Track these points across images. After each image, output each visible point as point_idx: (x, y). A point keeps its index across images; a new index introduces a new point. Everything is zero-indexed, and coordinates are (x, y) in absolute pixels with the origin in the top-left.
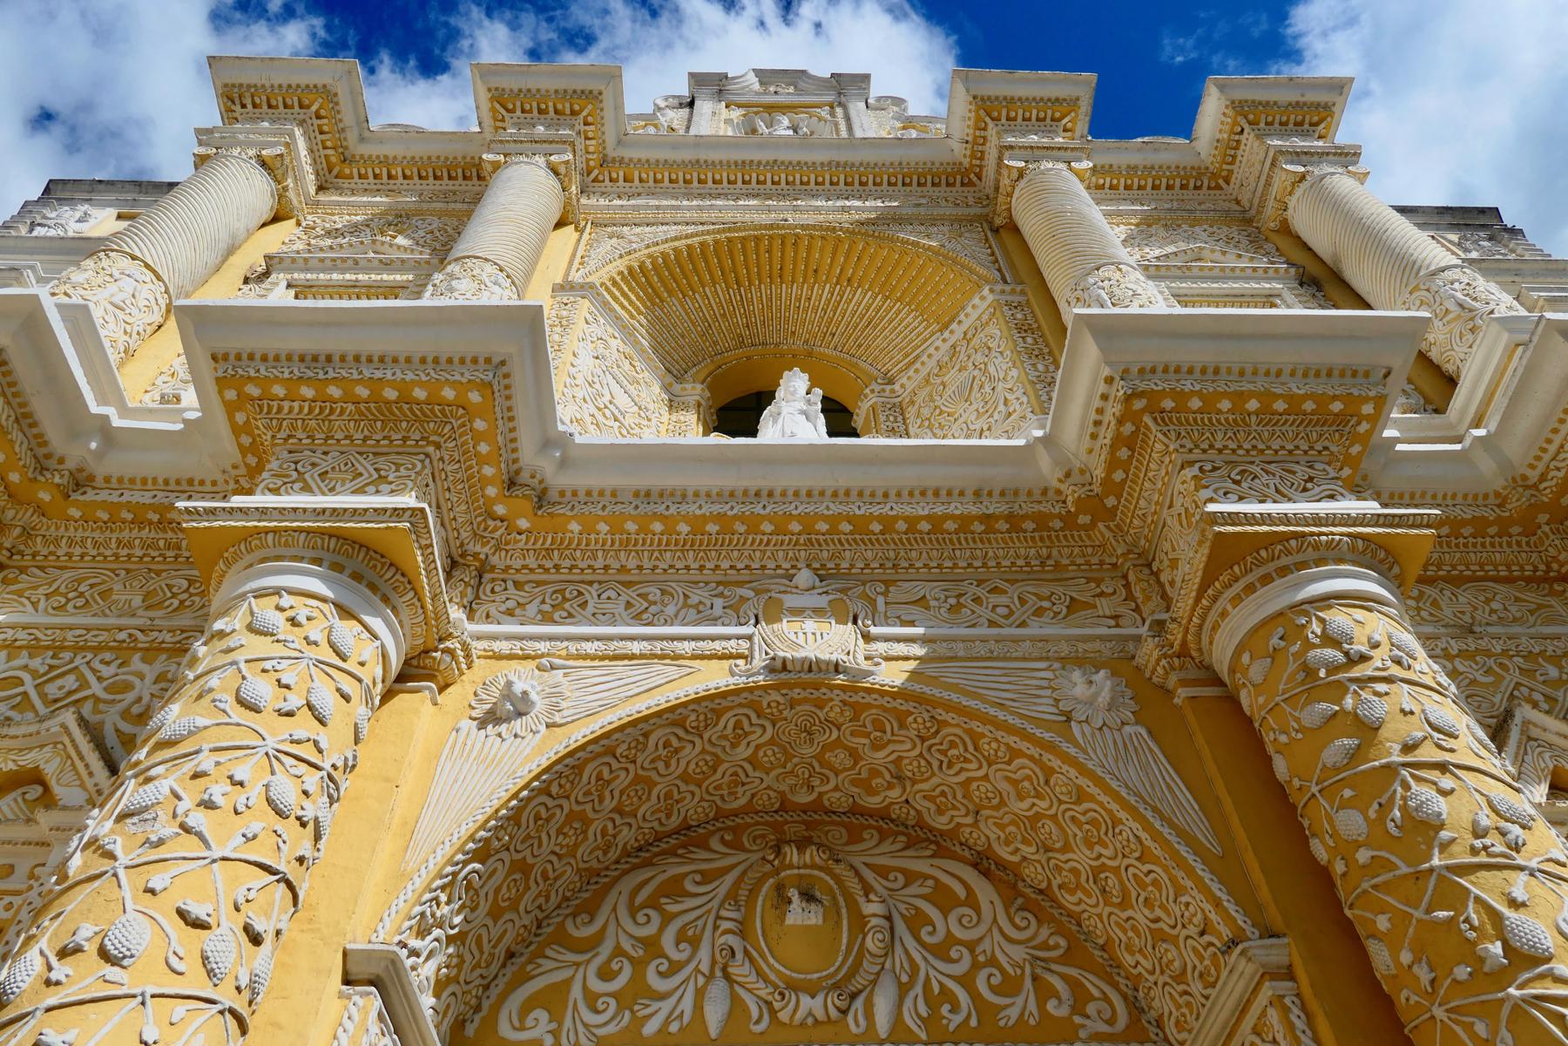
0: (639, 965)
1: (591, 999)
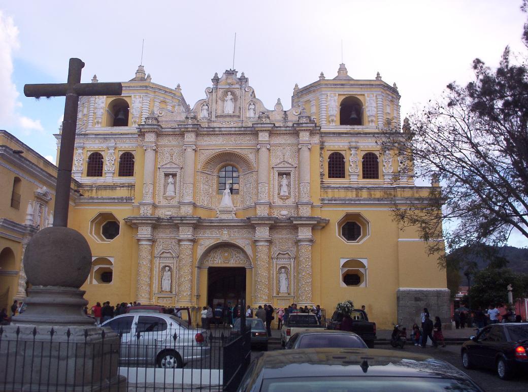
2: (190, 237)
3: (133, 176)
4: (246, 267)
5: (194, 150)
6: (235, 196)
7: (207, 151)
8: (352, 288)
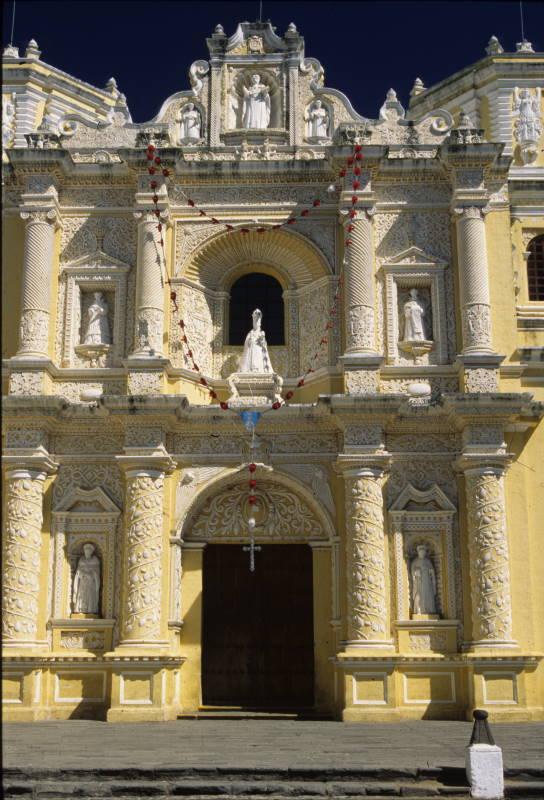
0: (220, 519)
1: (211, 526)
4: (312, 544)
6: (276, 349)
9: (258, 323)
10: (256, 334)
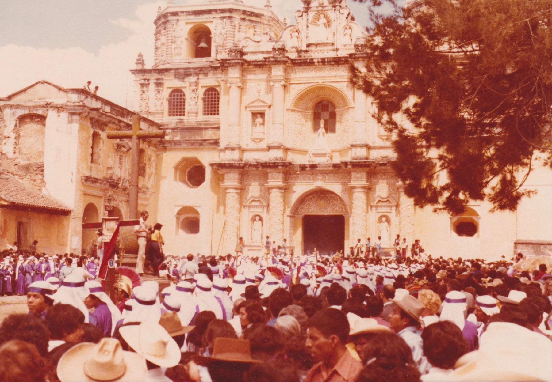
2: (280, 184)
3: (218, 114)
5: (282, 85)
7: (297, 86)
8: (465, 239)
9: (322, 125)
10: (322, 130)
